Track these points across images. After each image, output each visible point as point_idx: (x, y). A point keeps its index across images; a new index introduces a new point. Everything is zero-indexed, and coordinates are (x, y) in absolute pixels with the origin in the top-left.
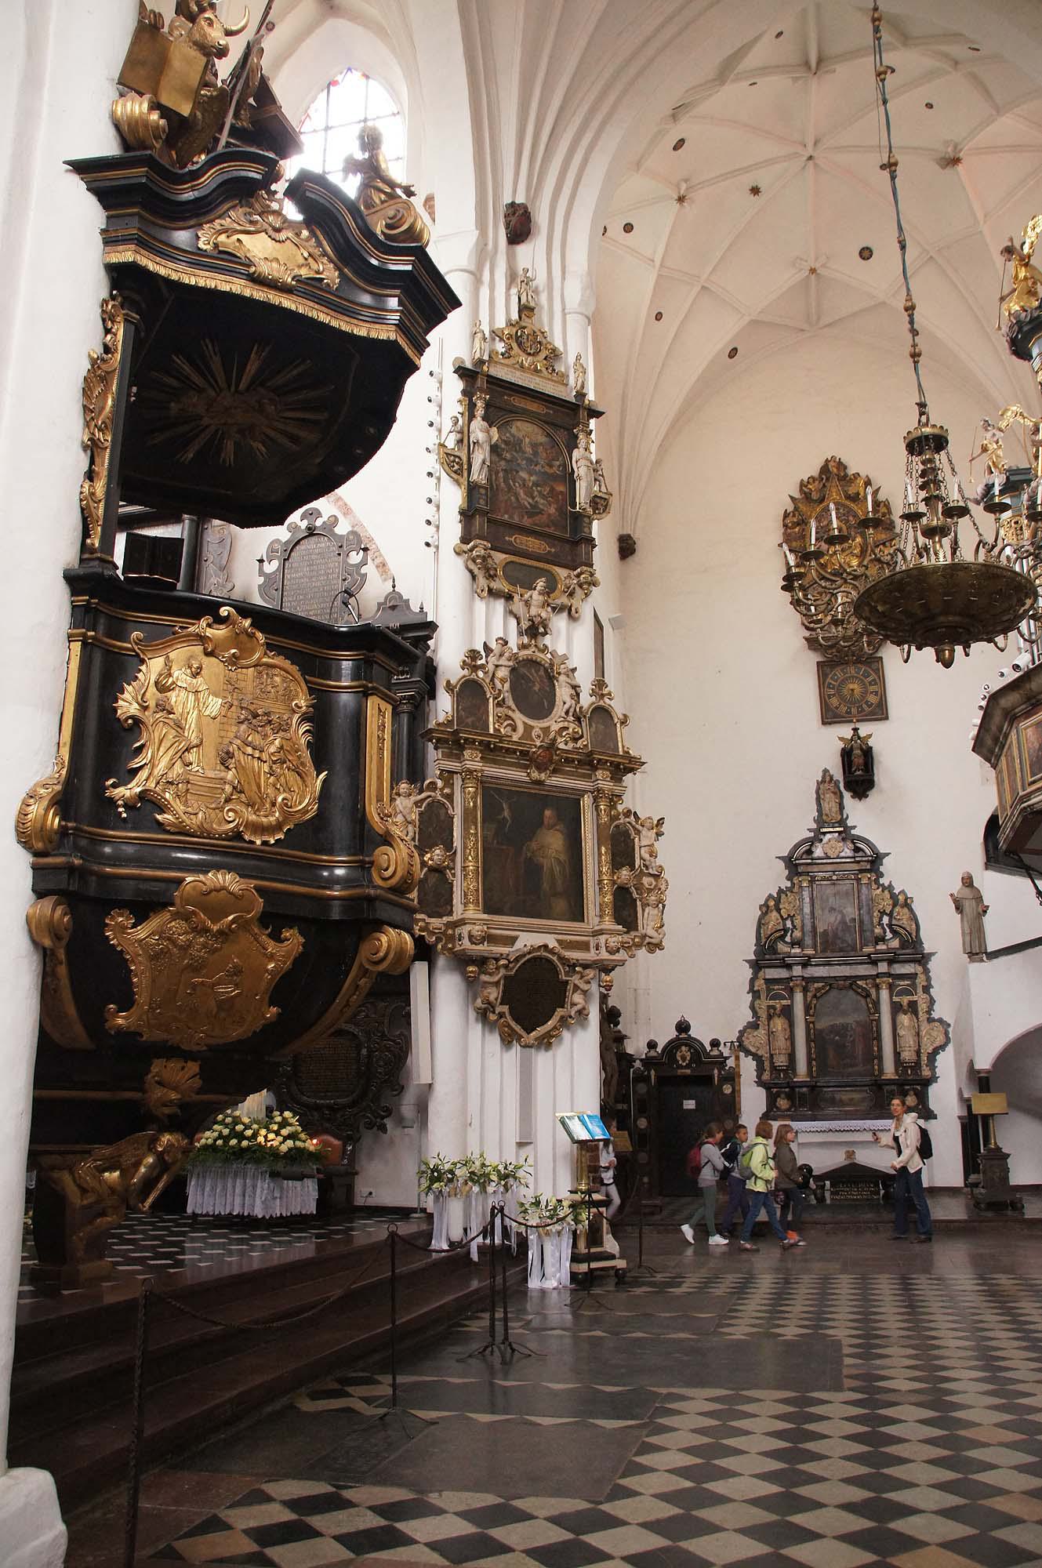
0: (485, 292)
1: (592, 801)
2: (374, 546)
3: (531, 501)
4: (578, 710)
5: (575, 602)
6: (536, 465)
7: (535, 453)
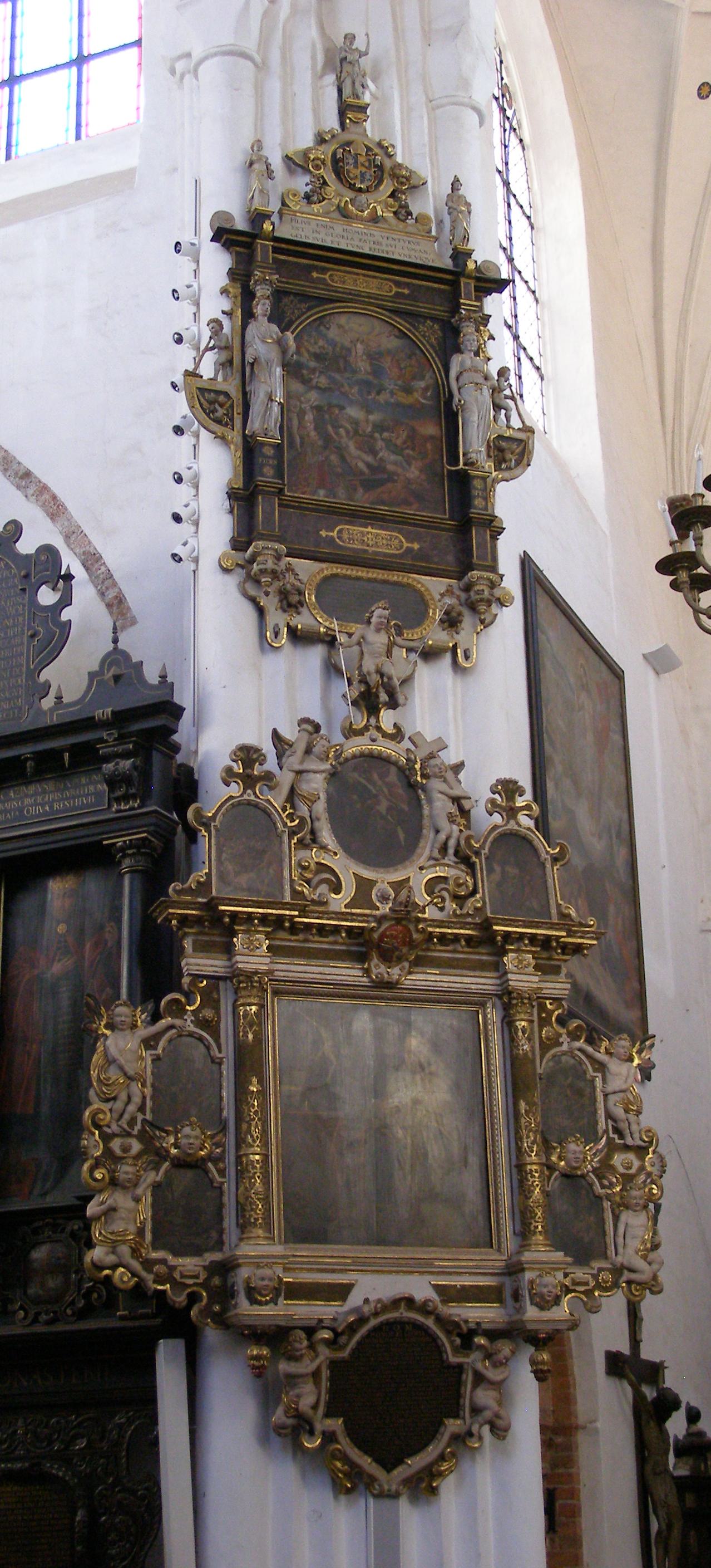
0: (274, 86)
1: (501, 1013)
2: (103, 569)
3: (369, 459)
4: (462, 842)
5: (464, 637)
6: (378, 393)
7: (377, 372)
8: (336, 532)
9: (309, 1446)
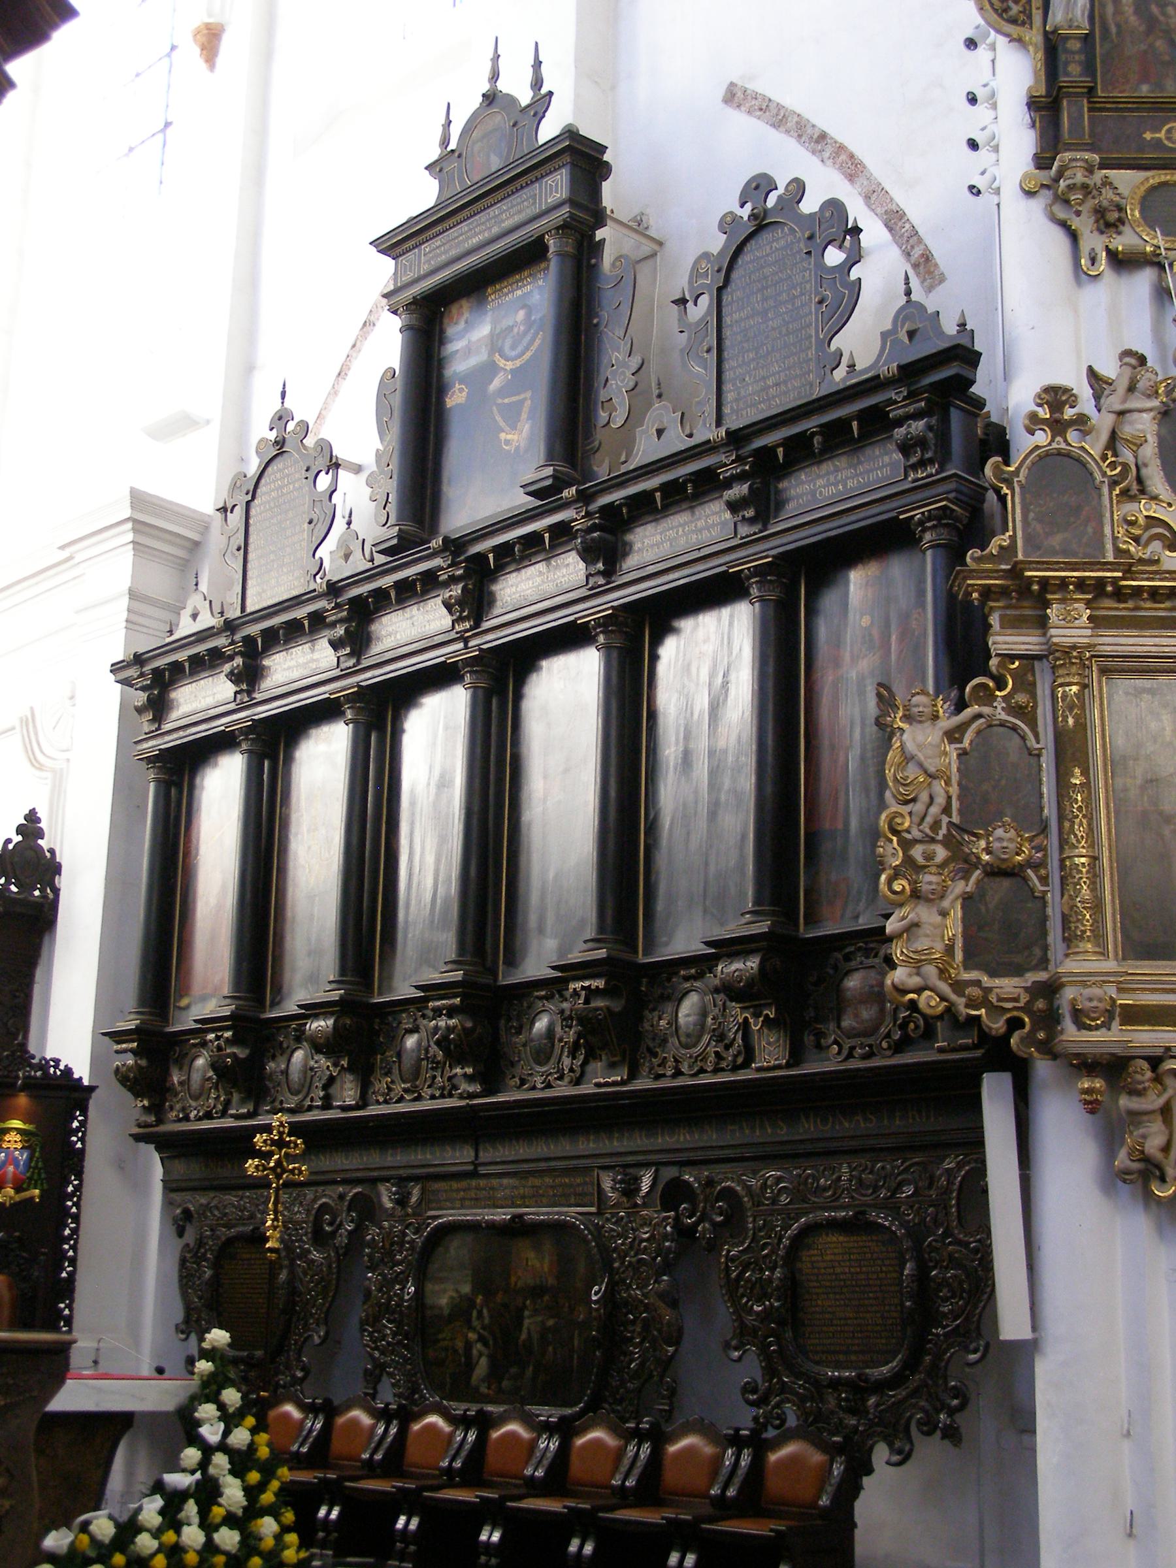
2: (907, 226)
8: (1163, 132)
9: (1161, 1194)
